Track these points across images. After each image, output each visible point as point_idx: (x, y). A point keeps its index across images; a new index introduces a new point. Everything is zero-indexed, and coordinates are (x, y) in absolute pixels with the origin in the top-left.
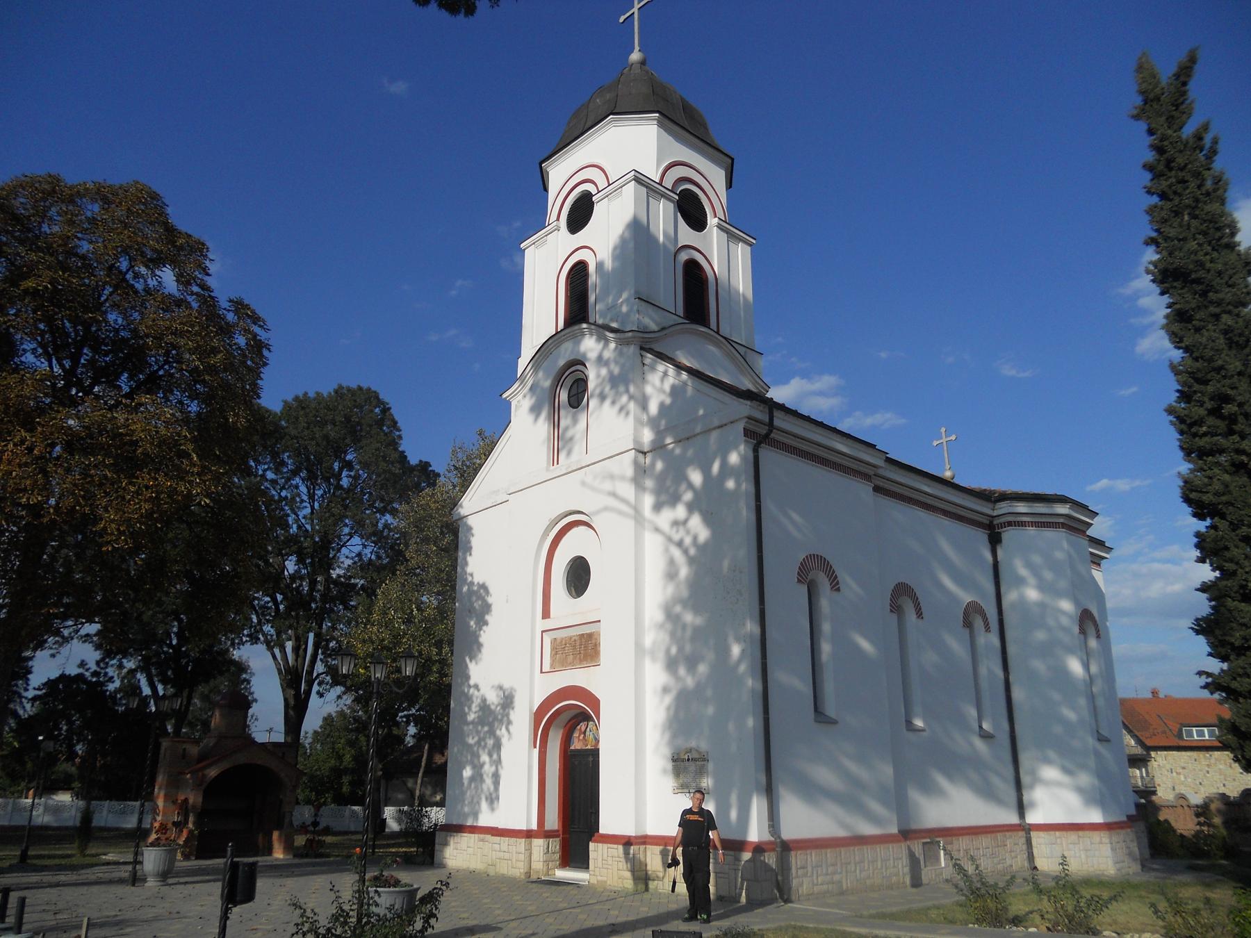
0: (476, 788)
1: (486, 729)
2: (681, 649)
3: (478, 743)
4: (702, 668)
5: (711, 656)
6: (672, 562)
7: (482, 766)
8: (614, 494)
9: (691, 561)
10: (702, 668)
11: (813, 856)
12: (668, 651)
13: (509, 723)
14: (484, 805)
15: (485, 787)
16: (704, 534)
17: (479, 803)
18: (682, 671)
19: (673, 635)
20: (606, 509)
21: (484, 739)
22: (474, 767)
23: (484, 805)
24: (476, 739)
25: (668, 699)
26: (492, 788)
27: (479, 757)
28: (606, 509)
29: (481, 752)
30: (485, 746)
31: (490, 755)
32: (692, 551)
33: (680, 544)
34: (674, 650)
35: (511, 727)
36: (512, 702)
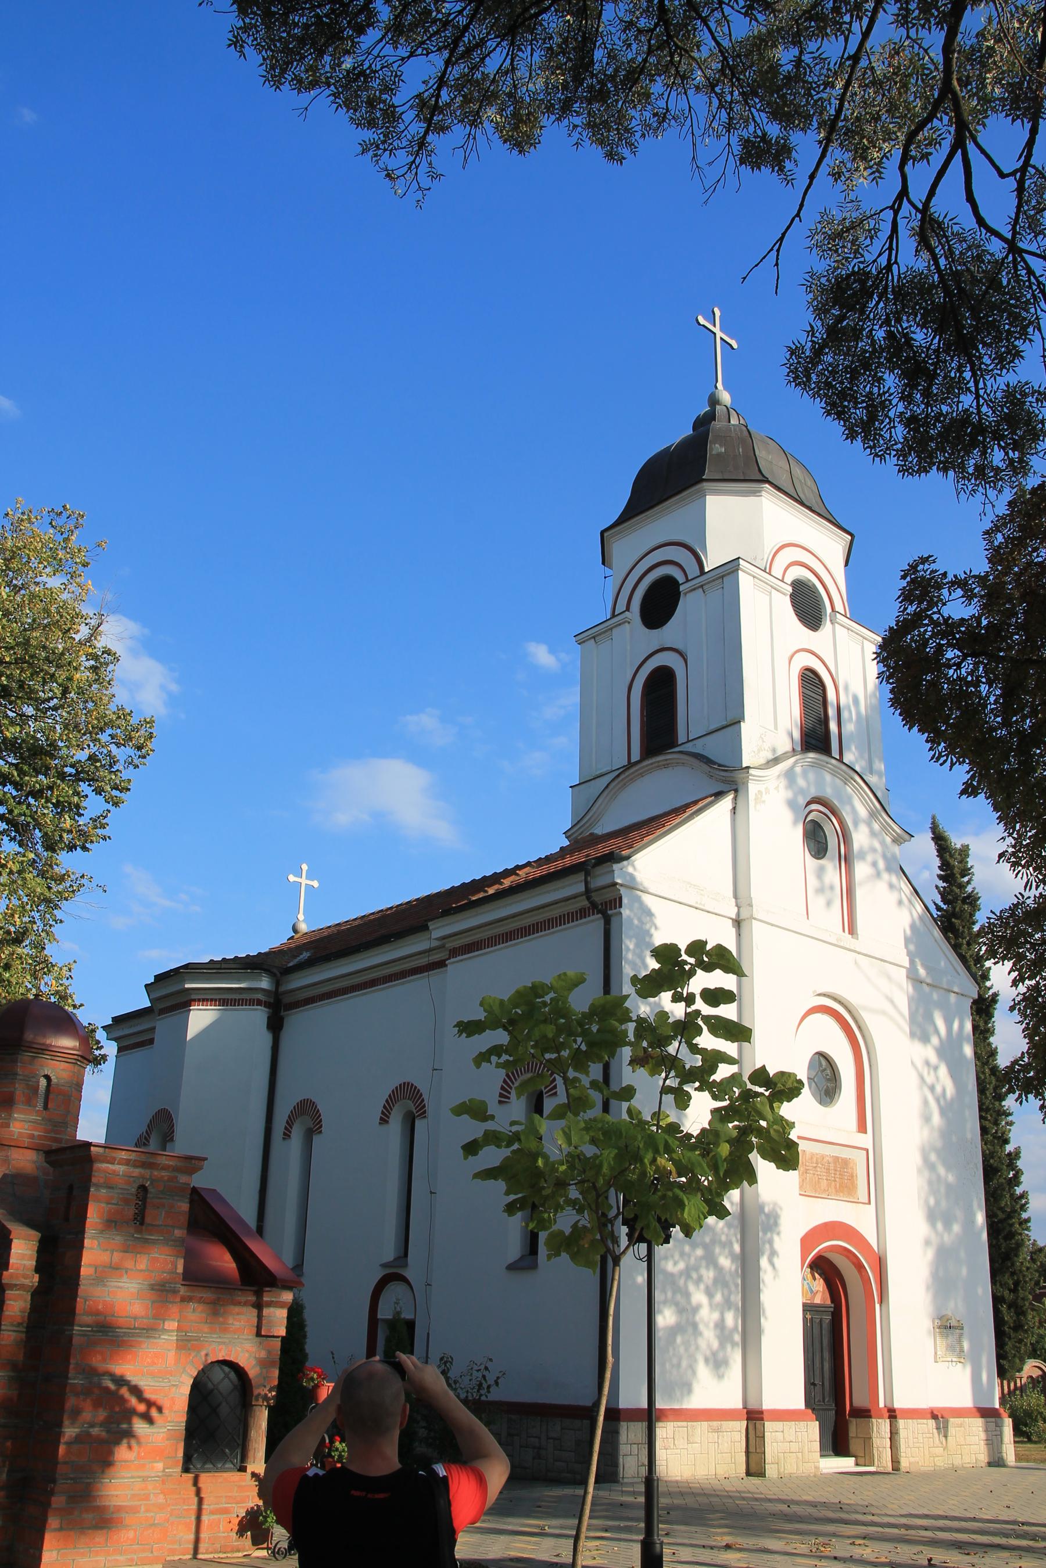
0: (687, 1344)
1: (699, 1252)
2: (937, 1202)
3: (687, 1273)
4: (956, 1228)
5: (959, 1214)
6: (926, 1102)
7: (696, 1309)
8: (892, 1002)
9: (943, 1112)
10: (956, 1228)
11: (779, 1425)
12: (926, 1202)
13: (773, 1253)
14: (703, 1371)
15: (702, 1343)
16: (950, 1091)
17: (692, 1368)
18: (940, 1226)
19: (930, 1183)
20: (884, 1013)
21: (696, 1269)
22: (681, 1311)
23: (703, 1371)
24: (681, 1265)
25: (930, 1254)
26: (715, 1344)
27: (687, 1295)
28: (884, 1013)
29: (691, 1288)
30: (700, 1279)
31: (710, 1294)
32: (942, 1102)
33: (932, 1088)
34: (932, 1201)
35: (775, 1260)
36: (776, 1224)
